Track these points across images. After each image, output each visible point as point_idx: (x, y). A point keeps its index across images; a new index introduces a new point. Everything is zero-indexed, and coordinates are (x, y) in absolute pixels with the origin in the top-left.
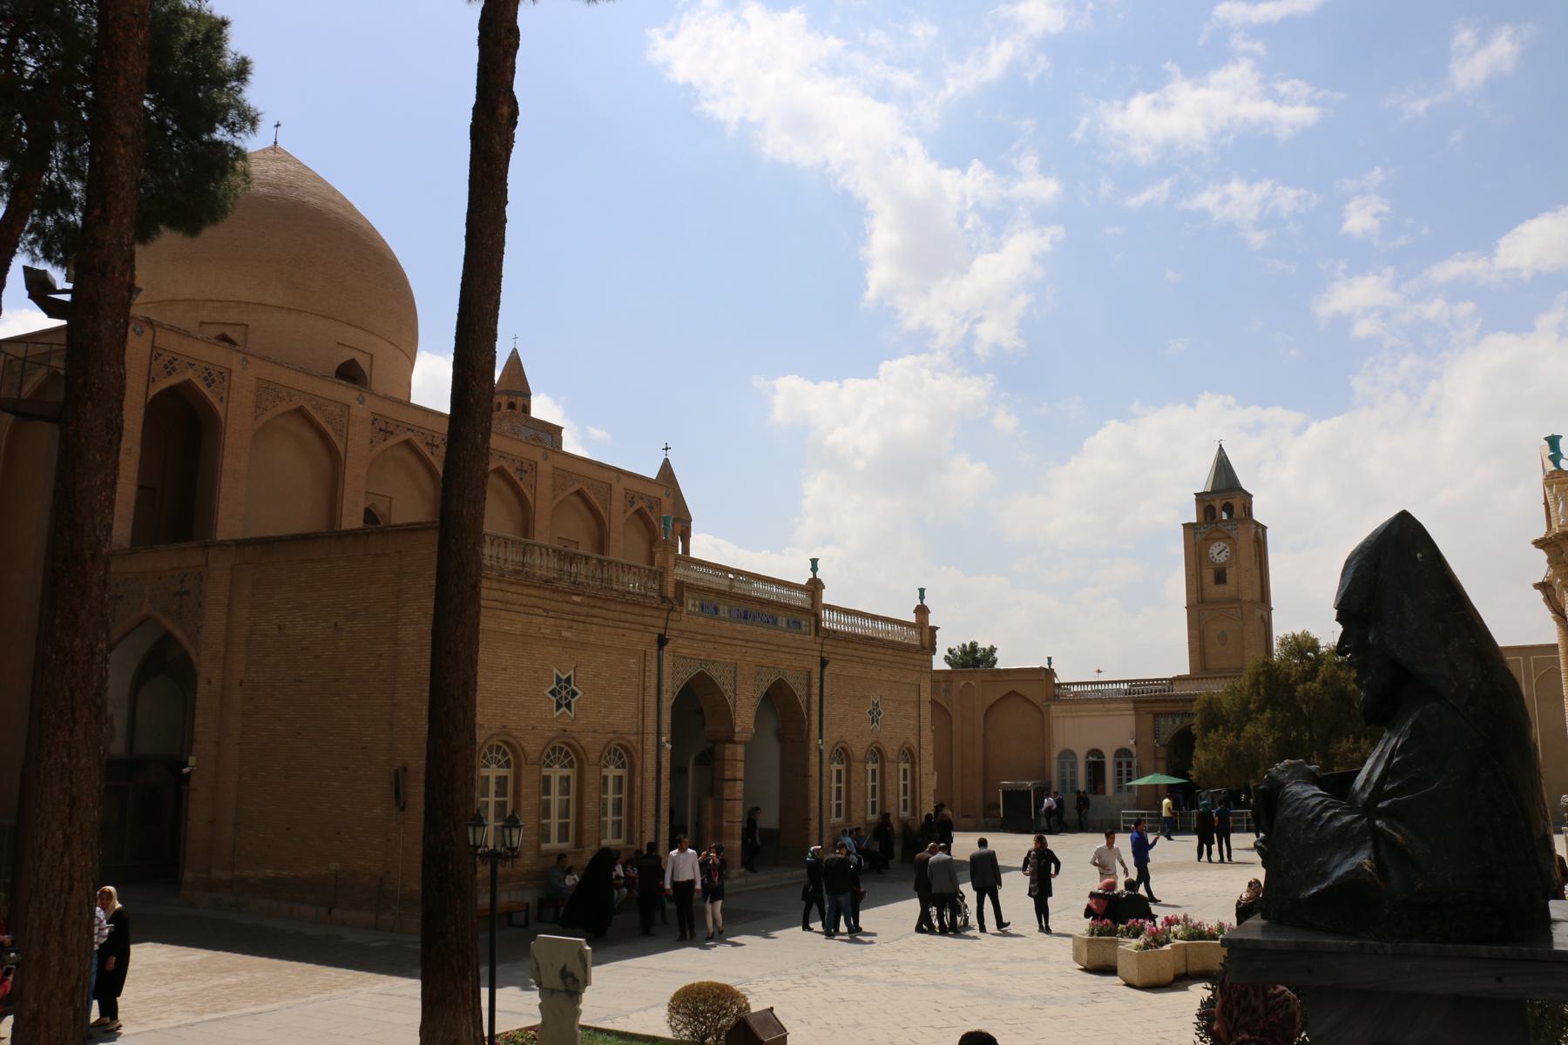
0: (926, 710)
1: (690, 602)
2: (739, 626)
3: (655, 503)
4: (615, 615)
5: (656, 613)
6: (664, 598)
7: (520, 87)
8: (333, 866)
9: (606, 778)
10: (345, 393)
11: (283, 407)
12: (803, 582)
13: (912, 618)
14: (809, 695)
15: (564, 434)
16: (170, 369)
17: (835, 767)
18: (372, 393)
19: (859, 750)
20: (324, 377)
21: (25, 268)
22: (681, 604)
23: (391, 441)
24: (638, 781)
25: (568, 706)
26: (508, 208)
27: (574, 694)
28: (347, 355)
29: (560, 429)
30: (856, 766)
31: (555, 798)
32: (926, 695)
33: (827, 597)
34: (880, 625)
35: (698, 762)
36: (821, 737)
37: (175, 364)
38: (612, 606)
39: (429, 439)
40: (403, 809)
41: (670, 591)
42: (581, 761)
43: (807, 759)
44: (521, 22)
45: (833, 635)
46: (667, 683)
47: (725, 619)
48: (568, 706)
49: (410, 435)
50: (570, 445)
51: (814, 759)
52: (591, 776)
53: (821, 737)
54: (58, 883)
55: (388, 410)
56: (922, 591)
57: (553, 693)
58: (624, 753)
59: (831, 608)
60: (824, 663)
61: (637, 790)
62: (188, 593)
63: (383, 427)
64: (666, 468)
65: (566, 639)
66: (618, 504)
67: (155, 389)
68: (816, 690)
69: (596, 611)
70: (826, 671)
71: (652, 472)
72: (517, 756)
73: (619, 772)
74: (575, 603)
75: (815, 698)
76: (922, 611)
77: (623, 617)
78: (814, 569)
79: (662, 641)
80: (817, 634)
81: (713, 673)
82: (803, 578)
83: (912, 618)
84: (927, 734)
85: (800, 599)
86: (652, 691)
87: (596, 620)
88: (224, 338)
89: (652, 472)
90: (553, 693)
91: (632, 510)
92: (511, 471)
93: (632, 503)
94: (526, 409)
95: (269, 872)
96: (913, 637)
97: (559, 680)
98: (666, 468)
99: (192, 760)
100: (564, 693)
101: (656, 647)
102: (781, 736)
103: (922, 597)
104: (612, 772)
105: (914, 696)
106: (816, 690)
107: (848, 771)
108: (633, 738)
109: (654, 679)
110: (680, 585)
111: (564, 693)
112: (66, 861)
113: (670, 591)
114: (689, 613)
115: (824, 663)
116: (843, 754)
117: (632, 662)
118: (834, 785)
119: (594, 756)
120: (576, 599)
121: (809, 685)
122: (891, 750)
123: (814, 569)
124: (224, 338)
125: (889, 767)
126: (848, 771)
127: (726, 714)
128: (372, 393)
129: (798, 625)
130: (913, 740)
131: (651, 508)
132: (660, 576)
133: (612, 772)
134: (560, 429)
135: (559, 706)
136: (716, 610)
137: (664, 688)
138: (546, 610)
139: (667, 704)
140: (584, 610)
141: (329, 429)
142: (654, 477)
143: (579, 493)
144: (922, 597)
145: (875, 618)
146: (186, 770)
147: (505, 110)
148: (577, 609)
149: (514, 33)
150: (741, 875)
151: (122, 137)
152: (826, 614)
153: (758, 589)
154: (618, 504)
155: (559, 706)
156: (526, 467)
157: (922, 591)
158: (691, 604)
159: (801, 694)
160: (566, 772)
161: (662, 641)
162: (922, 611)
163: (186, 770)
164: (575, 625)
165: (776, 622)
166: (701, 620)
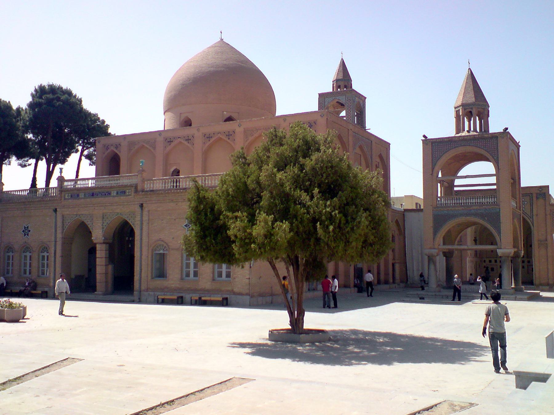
1: (66, 195)
2: (88, 200)
16: (108, 148)
27: (29, 231)
28: (183, 116)
39: (187, 138)
47: (81, 198)
60: (142, 206)
67: (104, 156)
90: (23, 231)
92: (224, 137)
100: (26, 231)
106: (138, 218)
115: (142, 206)
131: (310, 126)
136: (78, 195)
156: (231, 133)
161: (55, 211)
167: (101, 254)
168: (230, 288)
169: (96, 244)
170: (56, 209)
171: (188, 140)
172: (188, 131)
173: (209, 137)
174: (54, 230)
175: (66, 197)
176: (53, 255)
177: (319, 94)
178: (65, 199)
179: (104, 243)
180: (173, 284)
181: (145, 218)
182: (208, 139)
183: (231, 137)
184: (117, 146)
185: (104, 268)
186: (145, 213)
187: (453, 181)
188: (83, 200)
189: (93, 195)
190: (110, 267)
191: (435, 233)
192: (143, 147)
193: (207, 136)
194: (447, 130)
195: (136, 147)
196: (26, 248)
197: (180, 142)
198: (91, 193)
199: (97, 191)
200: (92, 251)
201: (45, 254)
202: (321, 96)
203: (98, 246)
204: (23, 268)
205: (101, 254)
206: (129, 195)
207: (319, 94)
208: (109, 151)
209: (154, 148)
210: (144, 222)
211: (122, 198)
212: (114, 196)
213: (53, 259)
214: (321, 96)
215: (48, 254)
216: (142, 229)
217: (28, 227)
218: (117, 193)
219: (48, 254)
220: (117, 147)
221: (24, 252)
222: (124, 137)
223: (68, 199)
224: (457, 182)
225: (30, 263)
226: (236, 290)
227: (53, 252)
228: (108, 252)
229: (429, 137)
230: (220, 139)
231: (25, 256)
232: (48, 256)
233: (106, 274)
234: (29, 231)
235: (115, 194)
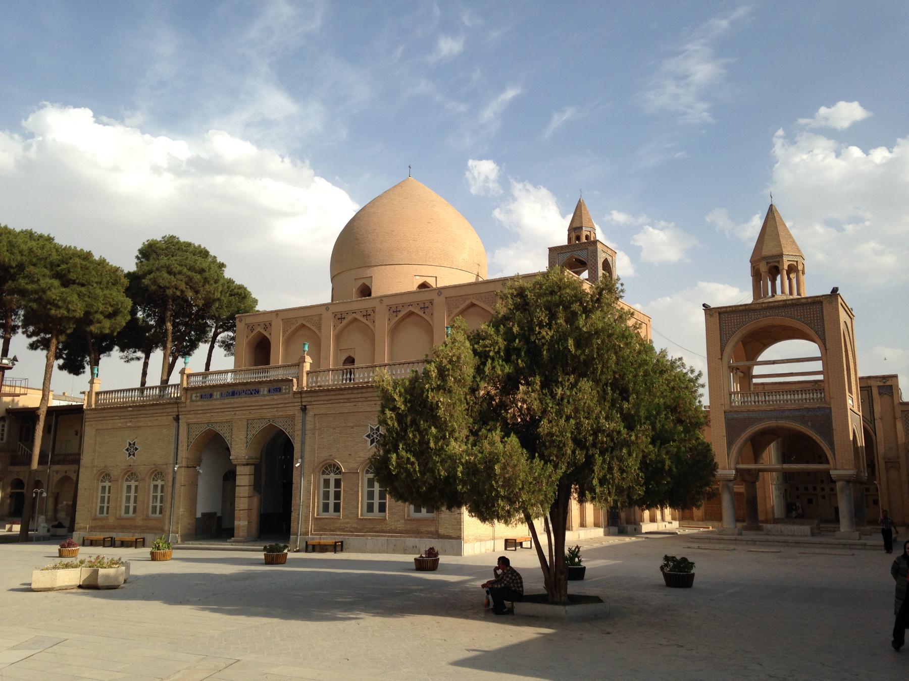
1: (194, 395)
2: (226, 401)
27: (136, 449)
28: (360, 283)
47: (216, 399)
49: (354, 315)
60: (304, 409)
68: (299, 426)
70: (310, 413)
81: (217, 428)
90: (127, 450)
92: (417, 311)
100: (132, 449)
106: (299, 426)
111: (132, 449)
115: (304, 409)
136: (211, 396)
141: (313, 328)
156: (427, 305)
161: (177, 419)
165: (258, 392)
166: (199, 403)
167: (244, 479)
168: (433, 529)
169: (235, 466)
170: (178, 416)
171: (366, 316)
172: (366, 303)
173: (397, 312)
174: (173, 447)
175: (194, 398)
176: (170, 484)
177: (551, 250)
178: (192, 401)
179: (247, 464)
180: (348, 523)
181: (309, 426)
182: (395, 314)
183: (427, 311)
184: (267, 326)
185: (246, 500)
186: (309, 417)
187: (750, 369)
188: (218, 402)
189: (233, 394)
190: (256, 500)
191: (730, 444)
192: (303, 326)
193: (394, 309)
194: (737, 293)
195: (294, 327)
196: (130, 474)
197: (355, 320)
198: (231, 391)
199: (239, 388)
200: (230, 476)
201: (159, 483)
202: (552, 250)
203: (239, 469)
204: (124, 504)
205: (244, 479)
206: (285, 394)
207: (551, 250)
208: (254, 333)
209: (320, 328)
210: (307, 432)
211: (276, 397)
212: (264, 396)
213: (170, 490)
214: (552, 250)
215: (163, 483)
216: (303, 443)
217: (134, 444)
218: (269, 391)
219: (163, 483)
220: (266, 328)
221: (127, 480)
222: (277, 313)
223: (196, 401)
224: (757, 370)
225: (136, 497)
226: (442, 531)
227: (171, 479)
228: (252, 477)
229: (713, 305)
230: (411, 313)
231: (129, 487)
232: (162, 487)
233: (249, 510)
234: (136, 449)
235: (266, 392)
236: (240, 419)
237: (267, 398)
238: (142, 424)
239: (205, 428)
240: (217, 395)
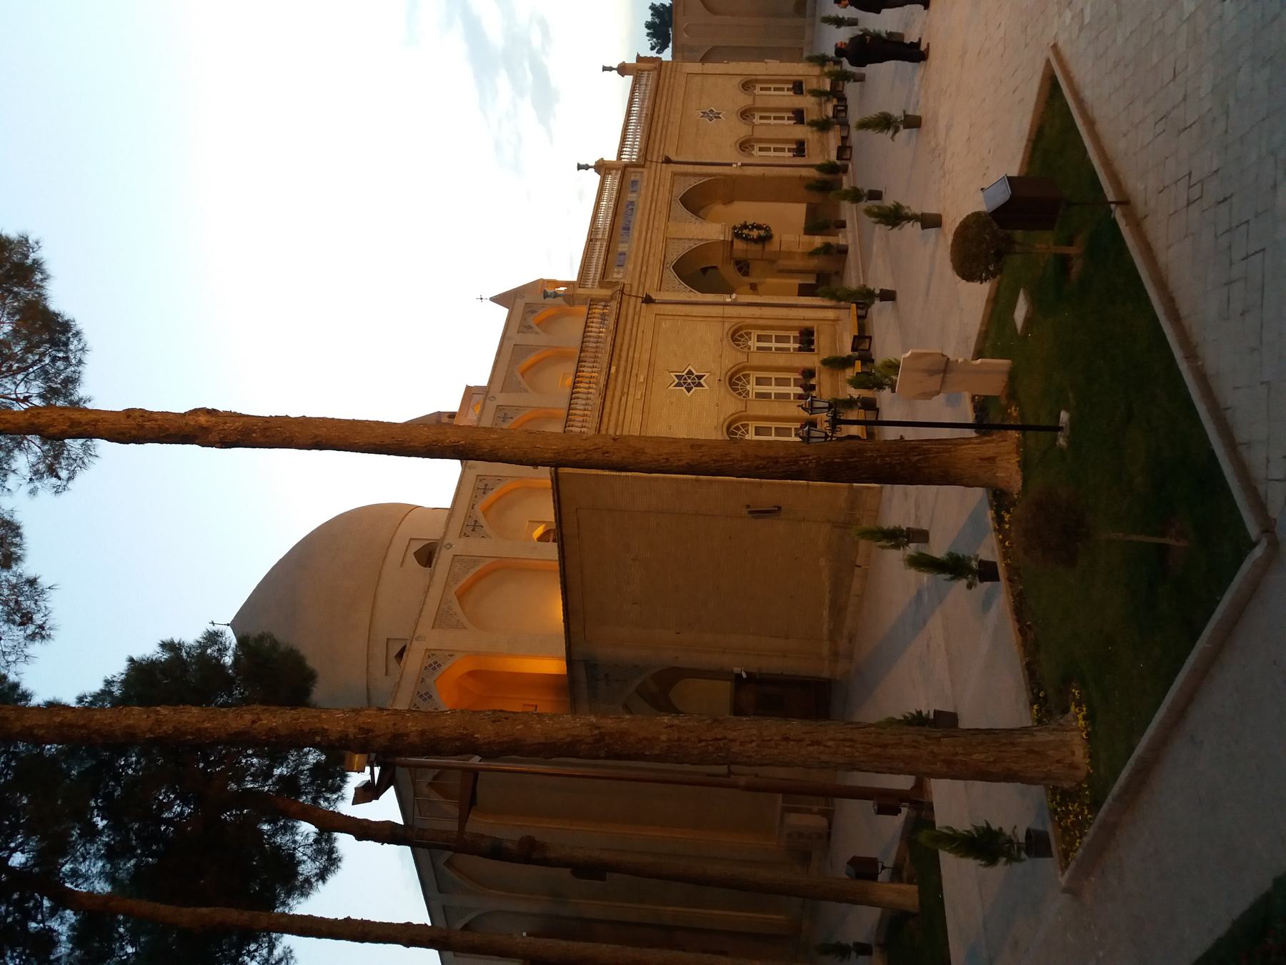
0: (710, 67)
1: (615, 275)
2: (636, 235)
3: (530, 309)
4: (627, 338)
5: (624, 305)
6: (612, 298)
7: (180, 406)
8: (823, 562)
9: (759, 348)
10: (443, 560)
11: (456, 607)
12: (597, 178)
13: (629, 79)
14: (695, 175)
15: (472, 384)
17: (756, 152)
18: (443, 538)
19: (743, 130)
20: (432, 576)
21: (355, 802)
22: (617, 283)
23: (482, 521)
24: (761, 322)
25: (700, 377)
26: (292, 415)
27: (690, 373)
28: (411, 560)
29: (468, 388)
30: (757, 135)
31: (773, 389)
32: (696, 67)
33: (611, 156)
34: (635, 109)
35: (746, 274)
36: (730, 165)
37: (422, 693)
38: (619, 340)
40: (780, 508)
41: (606, 292)
42: (744, 368)
43: (749, 177)
44: (119, 407)
45: (645, 151)
46: (683, 297)
48: (700, 377)
50: (483, 380)
51: (750, 171)
52: (756, 360)
53: (730, 165)
54: (847, 749)
55: (457, 525)
56: (605, 69)
57: (689, 390)
58: (737, 336)
59: (620, 152)
60: (668, 161)
61: (769, 323)
62: (606, 675)
63: (472, 528)
64: (500, 299)
65: (647, 379)
66: (530, 339)
69: (624, 354)
70: (673, 158)
71: (503, 312)
72: (740, 419)
73: (754, 337)
74: (617, 371)
75: (698, 169)
76: (623, 70)
77: (628, 332)
78: (587, 167)
79: (648, 300)
80: (643, 166)
81: (673, 257)
82: (593, 178)
83: (629, 79)
84: (733, 67)
85: (612, 181)
86: (688, 309)
87: (631, 354)
88: (400, 655)
89: (503, 312)
90: (689, 390)
91: (536, 329)
93: (530, 327)
94: (452, 415)
95: (825, 613)
96: (648, 80)
97: (678, 385)
98: (500, 299)
99: (737, 670)
100: (690, 381)
101: (653, 305)
102: (729, 200)
103: (610, 69)
104: (753, 343)
105: (698, 78)
106: (690, 168)
107: (760, 141)
108: (727, 326)
109: (680, 307)
110: (604, 283)
111: (690, 381)
112: (830, 743)
113: (606, 292)
114: (624, 277)
115: (668, 161)
116: (745, 146)
117: (665, 325)
118: (772, 153)
119: (741, 358)
120: (613, 369)
121: (685, 174)
122: (744, 100)
123: (587, 167)
124: (400, 655)
125: (758, 105)
126: (760, 141)
127: (706, 248)
128: (443, 538)
129: (635, 183)
130: (739, 79)
132: (592, 302)
133: (753, 343)
134: (468, 388)
135: (700, 385)
137: (687, 299)
138: (623, 394)
139: (699, 297)
140: (623, 364)
141: (474, 571)
142: (506, 311)
143: (523, 374)
144: (610, 69)
145: (629, 113)
146: (744, 676)
147: (203, 420)
148: (622, 369)
149: (129, 413)
150: (845, 237)
151: (254, 722)
152: (625, 158)
153: (604, 221)
154: (530, 339)
155: (700, 385)
157: (605, 69)
158: (616, 276)
159: (694, 182)
160: (753, 380)
161: (648, 300)
162: (623, 70)
163: (744, 676)
164: (634, 371)
166: (630, 267)
189: (628, 229)
196: (735, 380)
236: (667, 227)
237: (643, 192)
238: (646, 357)
239: (671, 274)
240: (622, 248)
